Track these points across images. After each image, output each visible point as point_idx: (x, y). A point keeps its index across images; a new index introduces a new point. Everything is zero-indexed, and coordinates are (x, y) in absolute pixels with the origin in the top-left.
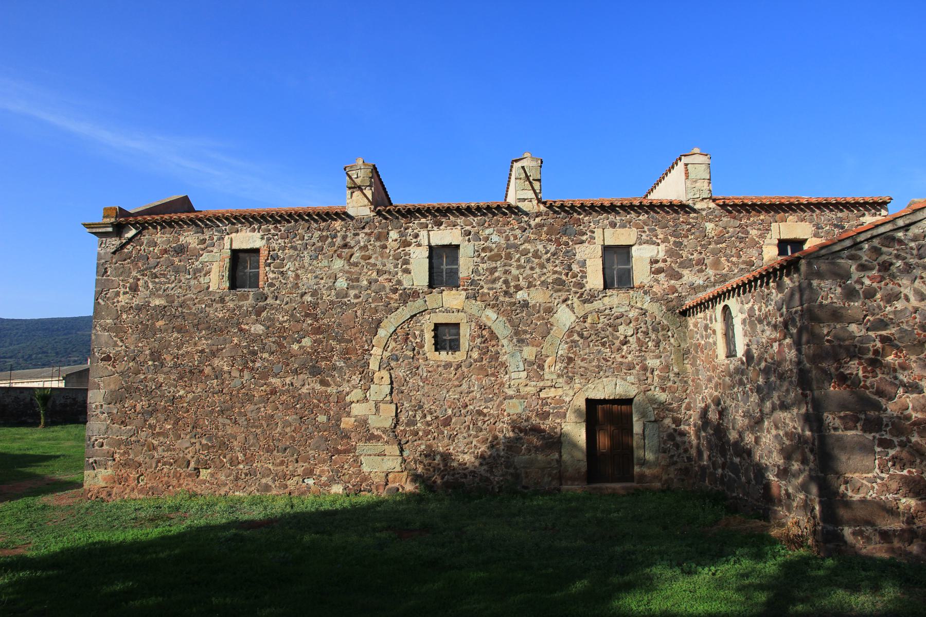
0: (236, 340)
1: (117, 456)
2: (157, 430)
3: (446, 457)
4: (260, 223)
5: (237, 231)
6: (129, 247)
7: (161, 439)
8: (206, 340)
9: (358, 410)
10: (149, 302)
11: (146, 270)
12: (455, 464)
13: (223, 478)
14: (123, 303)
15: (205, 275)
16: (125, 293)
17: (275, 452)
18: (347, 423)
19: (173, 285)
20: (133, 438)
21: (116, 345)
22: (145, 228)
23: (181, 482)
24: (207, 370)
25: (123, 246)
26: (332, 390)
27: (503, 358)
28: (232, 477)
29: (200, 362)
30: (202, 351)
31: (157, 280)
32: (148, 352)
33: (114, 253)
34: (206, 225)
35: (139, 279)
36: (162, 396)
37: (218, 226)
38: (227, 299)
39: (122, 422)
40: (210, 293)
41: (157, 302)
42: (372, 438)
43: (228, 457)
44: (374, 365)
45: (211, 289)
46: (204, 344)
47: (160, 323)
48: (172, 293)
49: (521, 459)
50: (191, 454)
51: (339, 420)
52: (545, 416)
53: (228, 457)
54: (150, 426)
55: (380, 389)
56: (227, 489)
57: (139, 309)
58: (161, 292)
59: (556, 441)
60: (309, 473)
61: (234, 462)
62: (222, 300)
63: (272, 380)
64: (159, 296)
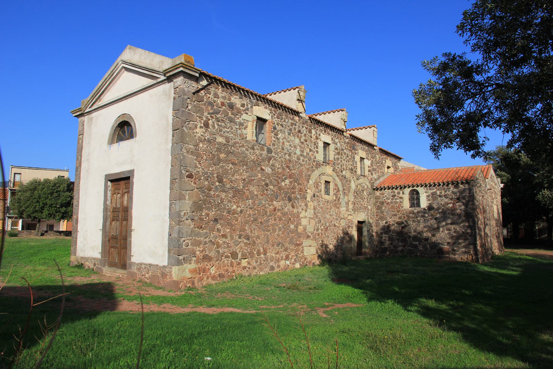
0: (259, 175)
1: (198, 253)
2: (222, 233)
3: (326, 246)
4: (269, 105)
5: (259, 106)
6: (202, 92)
7: (224, 239)
8: (247, 172)
9: (304, 222)
10: (216, 139)
11: (213, 114)
12: (328, 250)
13: (255, 264)
14: (199, 135)
15: (245, 129)
16: (201, 127)
17: (275, 246)
18: (300, 229)
19: (229, 130)
20: (207, 240)
21: (196, 167)
22: (212, 83)
23: (234, 268)
24: (247, 193)
25: (198, 91)
26: (295, 211)
27: (341, 200)
28: (258, 263)
29: (244, 187)
30: (244, 180)
31: (220, 123)
32: (215, 175)
33: (194, 94)
34: (245, 95)
35: (209, 119)
36: (225, 208)
37: (250, 98)
38: (255, 147)
39: (201, 227)
40: (247, 141)
41: (220, 139)
42: (308, 237)
43: (256, 250)
44: (309, 199)
45: (247, 139)
46: (245, 175)
47: (222, 156)
48: (228, 135)
49: (344, 246)
50: (239, 250)
51: (297, 228)
52: (349, 227)
53: (256, 250)
54: (218, 230)
55: (310, 212)
56: (256, 271)
57: (209, 141)
58: (222, 133)
59: (351, 238)
60: (287, 258)
61: (259, 253)
62: (253, 148)
63: (275, 203)
64: (221, 136)
